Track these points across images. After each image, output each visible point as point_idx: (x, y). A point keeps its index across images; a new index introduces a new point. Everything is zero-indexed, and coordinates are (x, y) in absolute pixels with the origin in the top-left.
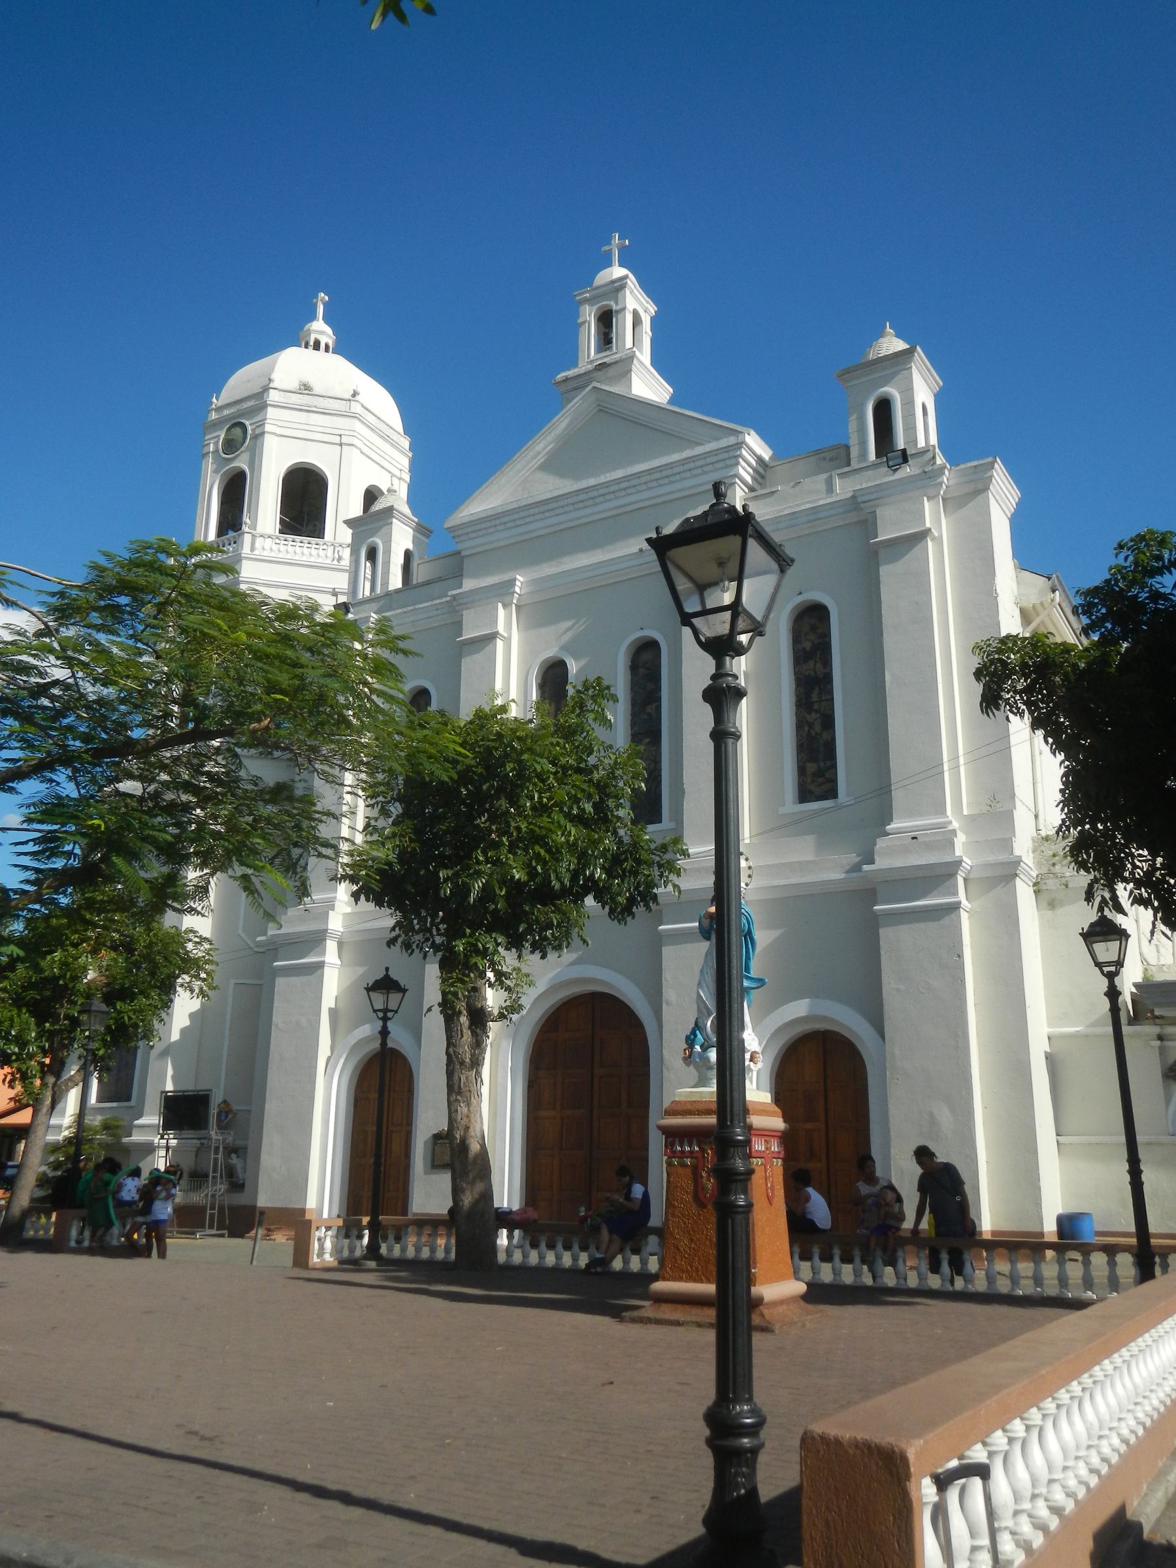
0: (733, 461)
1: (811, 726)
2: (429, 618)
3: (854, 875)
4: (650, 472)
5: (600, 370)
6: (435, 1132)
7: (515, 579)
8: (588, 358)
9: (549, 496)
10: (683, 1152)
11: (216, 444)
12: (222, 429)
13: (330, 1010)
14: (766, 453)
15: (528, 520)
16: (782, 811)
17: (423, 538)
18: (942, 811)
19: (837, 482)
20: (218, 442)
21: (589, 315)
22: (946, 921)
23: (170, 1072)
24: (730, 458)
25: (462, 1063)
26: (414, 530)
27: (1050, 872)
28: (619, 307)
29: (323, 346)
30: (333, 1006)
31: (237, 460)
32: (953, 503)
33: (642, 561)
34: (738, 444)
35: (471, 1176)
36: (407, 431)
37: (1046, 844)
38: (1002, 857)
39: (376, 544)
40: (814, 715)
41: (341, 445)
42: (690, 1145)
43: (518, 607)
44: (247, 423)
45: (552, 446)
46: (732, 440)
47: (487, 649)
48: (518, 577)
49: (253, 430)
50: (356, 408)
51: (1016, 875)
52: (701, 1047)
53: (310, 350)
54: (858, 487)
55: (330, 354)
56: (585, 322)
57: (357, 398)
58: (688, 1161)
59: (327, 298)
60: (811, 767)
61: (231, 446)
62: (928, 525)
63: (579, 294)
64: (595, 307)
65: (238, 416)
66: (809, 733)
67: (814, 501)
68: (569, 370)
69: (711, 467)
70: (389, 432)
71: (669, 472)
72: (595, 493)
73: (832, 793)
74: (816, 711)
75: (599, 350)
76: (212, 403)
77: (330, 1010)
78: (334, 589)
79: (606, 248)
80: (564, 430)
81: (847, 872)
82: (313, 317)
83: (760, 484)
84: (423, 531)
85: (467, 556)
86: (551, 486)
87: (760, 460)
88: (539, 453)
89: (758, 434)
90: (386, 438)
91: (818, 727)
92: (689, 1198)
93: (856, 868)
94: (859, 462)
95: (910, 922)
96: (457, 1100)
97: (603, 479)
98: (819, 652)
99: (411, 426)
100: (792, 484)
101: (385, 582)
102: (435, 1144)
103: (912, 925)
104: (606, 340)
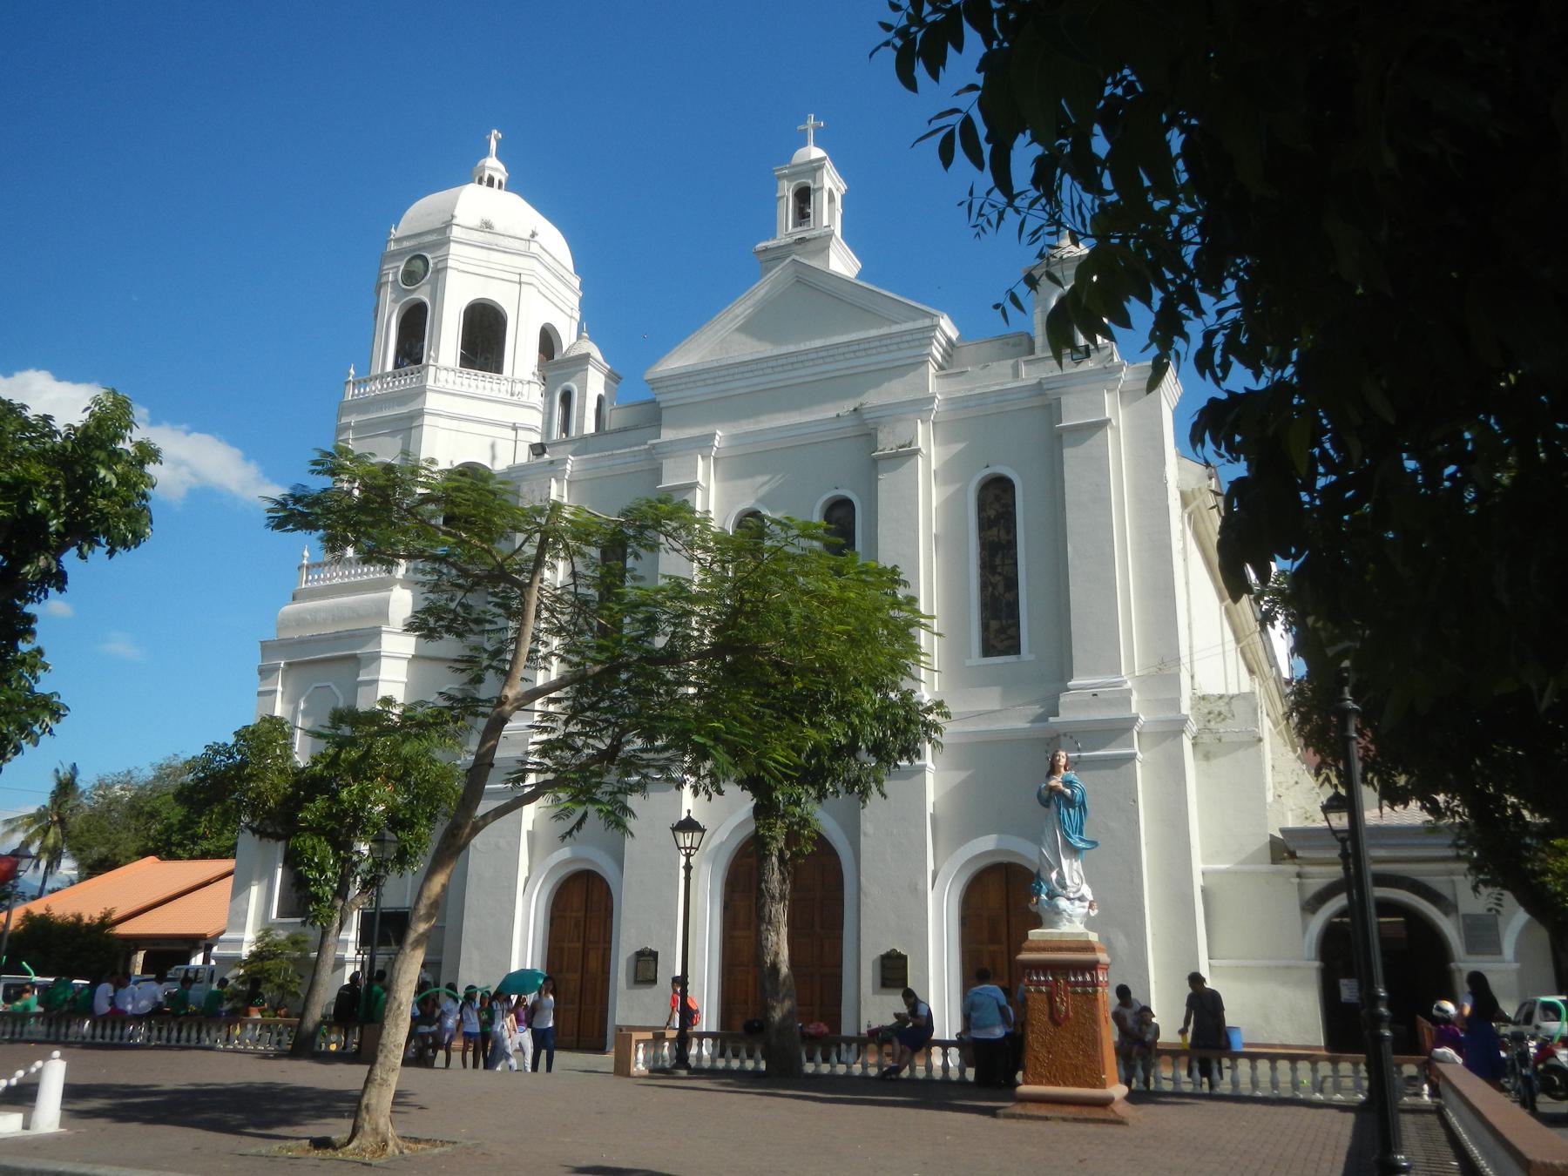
0: (928, 341)
1: (994, 586)
3: (1037, 725)
7: (715, 434)
8: (787, 230)
9: (749, 358)
10: (1039, 981)
11: (396, 274)
12: (402, 260)
13: (528, 832)
14: (953, 333)
15: (727, 378)
16: (968, 663)
17: (610, 382)
18: (1119, 672)
19: (1023, 369)
20: (397, 272)
21: (787, 190)
22: (1123, 769)
24: (924, 338)
25: (773, 897)
26: (606, 376)
27: (1206, 728)
28: (816, 186)
29: (496, 182)
30: (531, 829)
32: (1127, 397)
35: (781, 995)
36: (579, 269)
37: (1202, 703)
38: (1171, 715)
39: (569, 386)
40: (998, 578)
41: (520, 283)
42: (1045, 976)
43: (715, 459)
44: (429, 256)
45: (751, 310)
46: (927, 322)
48: (718, 432)
49: (436, 264)
50: (534, 248)
51: (1183, 731)
52: (1047, 895)
53: (484, 188)
54: (1044, 375)
55: (502, 192)
56: (783, 197)
57: (536, 238)
58: (1044, 989)
59: (500, 136)
60: (994, 624)
61: (411, 277)
62: (1107, 415)
63: (779, 170)
64: (794, 183)
66: (993, 594)
67: (1002, 384)
68: (768, 240)
69: (906, 345)
70: (563, 272)
71: (867, 346)
72: (795, 359)
73: (1015, 649)
74: (1000, 574)
75: (795, 226)
76: (390, 233)
77: (528, 832)
79: (802, 127)
81: (1032, 721)
82: (486, 153)
83: (947, 362)
84: (613, 378)
85: (667, 407)
86: (751, 349)
87: (949, 340)
89: (950, 317)
90: (561, 278)
91: (1001, 589)
92: (1045, 1019)
93: (1042, 718)
95: (1089, 770)
96: (767, 929)
97: (803, 347)
98: (1002, 521)
99: (582, 264)
100: (981, 366)
101: (581, 426)
103: (1093, 772)
104: (802, 215)
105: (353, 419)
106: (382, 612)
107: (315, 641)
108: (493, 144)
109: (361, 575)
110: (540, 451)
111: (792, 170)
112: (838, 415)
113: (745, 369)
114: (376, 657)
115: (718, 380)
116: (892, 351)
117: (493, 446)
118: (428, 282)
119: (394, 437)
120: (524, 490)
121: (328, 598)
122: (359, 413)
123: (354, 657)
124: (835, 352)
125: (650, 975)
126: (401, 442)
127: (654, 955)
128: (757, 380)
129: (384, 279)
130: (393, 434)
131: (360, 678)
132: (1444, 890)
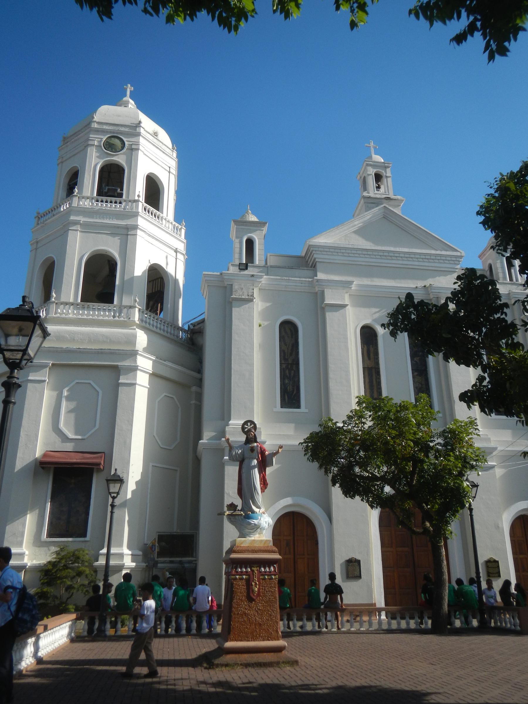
4: (420, 254)
5: (387, 200)
6: (347, 559)
7: (353, 282)
12: (105, 136)
20: (101, 141)
21: (372, 171)
23: (127, 518)
31: (116, 157)
34: (461, 256)
41: (169, 172)
44: (125, 139)
45: (362, 224)
47: (341, 311)
56: (371, 175)
65: (117, 133)
76: (93, 118)
78: (176, 249)
80: (369, 219)
82: (125, 96)
85: (319, 262)
88: (355, 225)
94: (503, 280)
97: (398, 249)
102: (348, 565)
105: (82, 219)
106: (132, 340)
107: (80, 352)
108: (128, 93)
109: (79, 314)
110: (244, 267)
111: (375, 164)
112: (417, 287)
113: (366, 253)
114: (134, 369)
115: (350, 255)
117: (167, 257)
119: (114, 237)
120: (236, 287)
121: (81, 326)
124: (413, 256)
125: (357, 573)
126: (119, 241)
127: (358, 562)
128: (371, 260)
129: (90, 143)
130: (113, 234)
131: (120, 381)
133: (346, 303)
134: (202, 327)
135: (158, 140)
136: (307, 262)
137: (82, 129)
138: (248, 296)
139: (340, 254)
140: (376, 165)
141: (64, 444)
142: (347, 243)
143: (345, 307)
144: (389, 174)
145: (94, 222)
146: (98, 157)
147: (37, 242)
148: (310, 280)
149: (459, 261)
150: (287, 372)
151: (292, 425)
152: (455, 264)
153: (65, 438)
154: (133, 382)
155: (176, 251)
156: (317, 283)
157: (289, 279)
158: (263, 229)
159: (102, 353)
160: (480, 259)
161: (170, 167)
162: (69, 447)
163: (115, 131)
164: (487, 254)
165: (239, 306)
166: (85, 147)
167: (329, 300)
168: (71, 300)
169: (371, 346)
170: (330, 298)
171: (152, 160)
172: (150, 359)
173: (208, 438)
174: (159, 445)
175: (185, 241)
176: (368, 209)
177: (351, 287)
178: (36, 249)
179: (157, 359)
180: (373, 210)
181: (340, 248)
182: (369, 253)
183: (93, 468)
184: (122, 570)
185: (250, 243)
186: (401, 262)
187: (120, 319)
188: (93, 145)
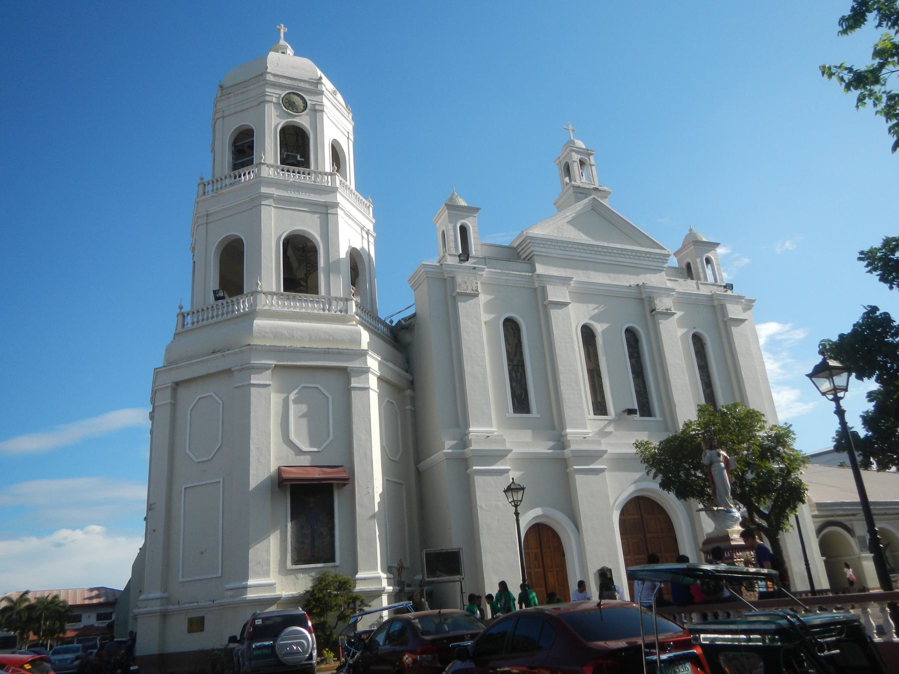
2: (516, 280)
5: (595, 190)
7: (573, 278)
19: (701, 286)
20: (279, 98)
21: (576, 157)
33: (627, 290)
44: (307, 98)
45: (574, 215)
56: (576, 162)
65: (297, 89)
78: (368, 230)
97: (611, 245)
108: (282, 35)
112: (630, 286)
116: (621, 257)
118: (307, 114)
119: (314, 214)
120: (459, 280)
121: (298, 321)
122: (278, 188)
123: (344, 370)
132: (849, 526)
133: (568, 301)
134: (413, 323)
135: (336, 99)
136: (519, 253)
137: (250, 79)
138: (473, 290)
139: (556, 247)
140: (579, 151)
141: (298, 457)
142: (560, 235)
143: (568, 305)
144: (593, 162)
145: (289, 197)
146: (277, 116)
147: (207, 215)
148: (530, 274)
149: (667, 260)
150: (514, 374)
151: (529, 432)
152: (663, 262)
153: (299, 452)
154: (366, 386)
155: (368, 233)
156: (538, 279)
157: (510, 273)
158: (475, 215)
159: (328, 353)
160: (676, 257)
161: (348, 133)
162: (305, 461)
163: (295, 87)
164: (684, 253)
165: (464, 301)
166: (260, 103)
167: (552, 298)
168: (274, 290)
169: (590, 347)
170: (555, 294)
171: (333, 122)
172: (376, 359)
173: (449, 447)
174: (388, 456)
175: (374, 221)
176: (578, 200)
177: (570, 284)
178: (207, 224)
179: (384, 362)
180: (583, 201)
181: (557, 241)
182: (584, 248)
183: (332, 483)
184: (381, 595)
185: (464, 230)
186: (614, 259)
187: (331, 313)
188: (271, 102)
